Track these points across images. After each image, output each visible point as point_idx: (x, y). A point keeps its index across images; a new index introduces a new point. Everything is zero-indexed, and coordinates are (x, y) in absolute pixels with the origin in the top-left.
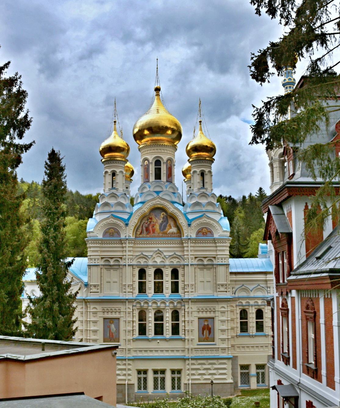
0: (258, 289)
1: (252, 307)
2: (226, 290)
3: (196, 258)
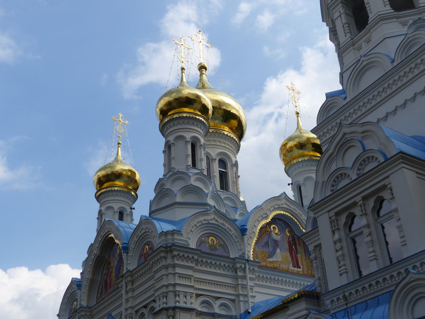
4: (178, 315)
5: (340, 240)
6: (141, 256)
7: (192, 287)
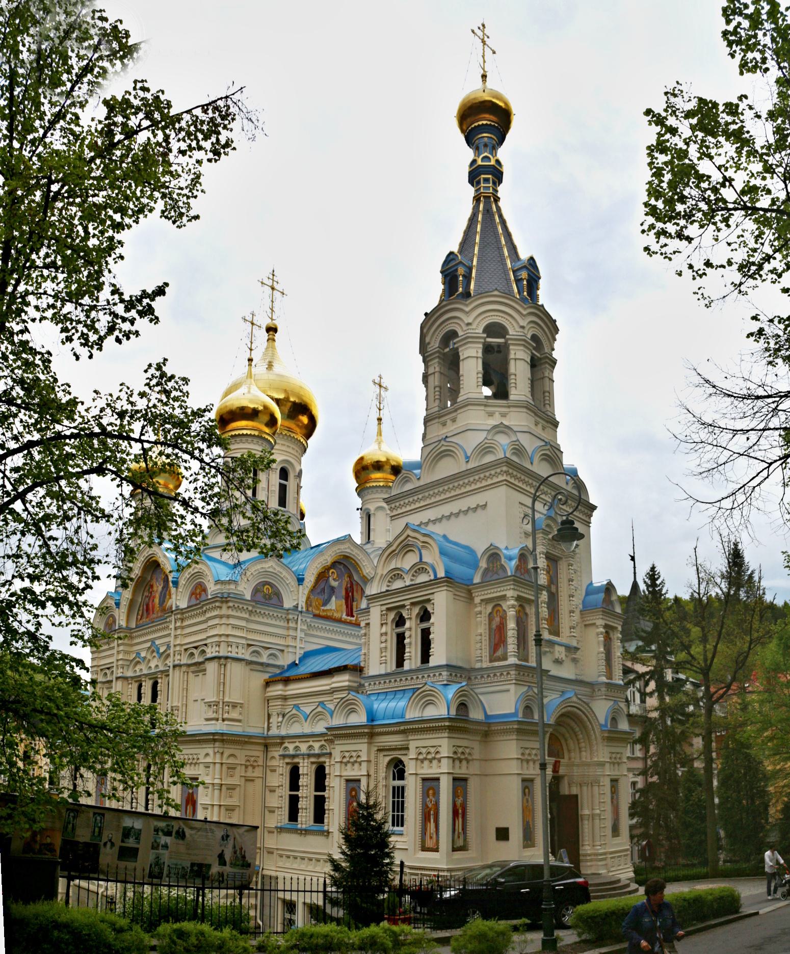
0: (316, 716)
2: (214, 716)
4: (228, 665)
5: (386, 634)
6: (192, 594)
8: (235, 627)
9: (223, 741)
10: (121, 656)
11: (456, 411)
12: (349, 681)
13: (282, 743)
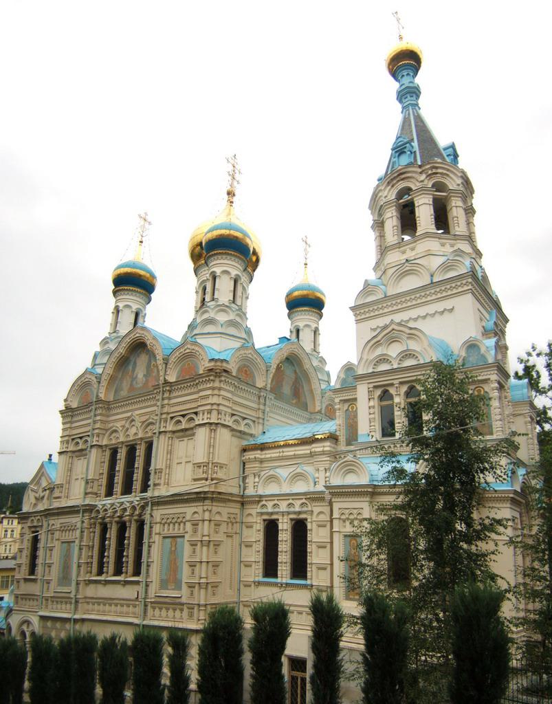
1: (283, 515)
2: (205, 476)
3: (172, 418)
5: (374, 407)
7: (231, 408)
8: (224, 398)
9: (212, 499)
10: (98, 425)
11: (415, 242)
12: (329, 446)
13: (259, 502)
